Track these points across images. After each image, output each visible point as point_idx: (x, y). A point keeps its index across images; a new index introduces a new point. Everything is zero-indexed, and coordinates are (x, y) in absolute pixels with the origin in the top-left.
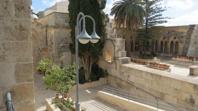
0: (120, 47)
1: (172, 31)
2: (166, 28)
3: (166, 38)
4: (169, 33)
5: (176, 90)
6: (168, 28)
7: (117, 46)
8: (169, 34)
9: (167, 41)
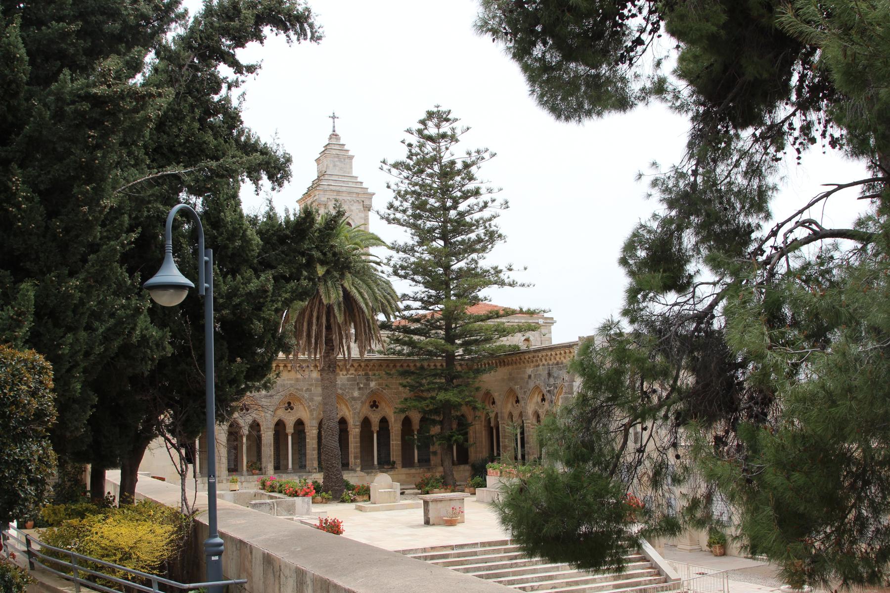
4: (549, 375)
8: (552, 381)
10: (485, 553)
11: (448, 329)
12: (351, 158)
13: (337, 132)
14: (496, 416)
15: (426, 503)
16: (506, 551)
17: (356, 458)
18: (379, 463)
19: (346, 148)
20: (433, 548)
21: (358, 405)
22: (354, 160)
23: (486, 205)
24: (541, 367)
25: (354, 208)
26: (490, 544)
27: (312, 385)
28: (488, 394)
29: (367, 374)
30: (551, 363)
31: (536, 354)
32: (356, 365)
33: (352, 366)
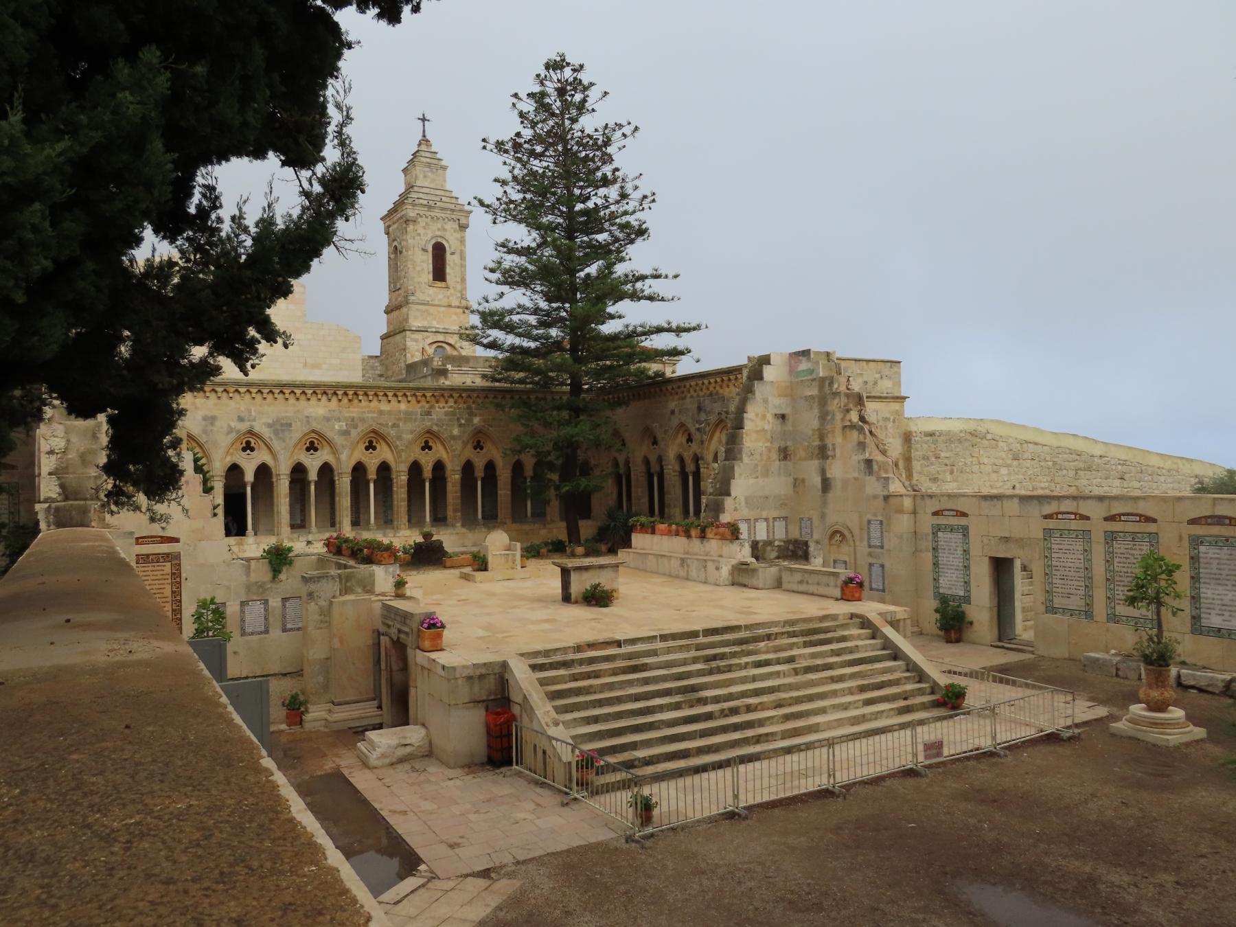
4: (700, 409)
7: (51, 452)
8: (703, 416)
10: (669, 650)
11: (573, 350)
12: (444, 168)
13: (428, 137)
14: (627, 462)
15: (565, 573)
16: (699, 647)
17: (455, 511)
18: (483, 518)
19: (438, 156)
20: (591, 646)
21: (458, 446)
22: (448, 172)
24: (688, 400)
25: (447, 227)
26: (674, 637)
27: (399, 419)
28: (616, 433)
29: (469, 408)
31: (682, 384)
32: (456, 395)
33: (451, 396)
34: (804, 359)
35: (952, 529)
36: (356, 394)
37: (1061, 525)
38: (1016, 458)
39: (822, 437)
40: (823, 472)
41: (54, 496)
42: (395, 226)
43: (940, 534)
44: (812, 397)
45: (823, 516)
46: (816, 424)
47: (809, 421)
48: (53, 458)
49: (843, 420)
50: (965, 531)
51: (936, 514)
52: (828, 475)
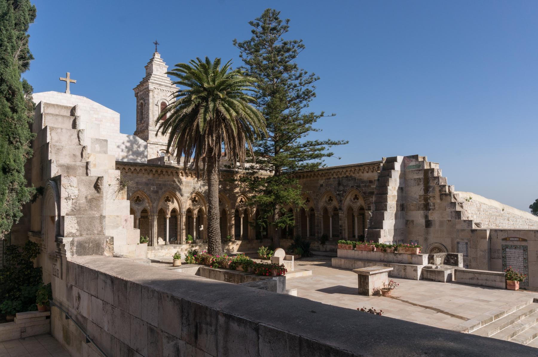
0: (83, 201)
1: (347, 177)
2: (332, 172)
3: (334, 199)
4: (339, 184)
5: (152, 330)
6: (336, 171)
8: (341, 188)
9: (338, 207)
23: (300, 76)
30: (340, 176)
34: (414, 160)
35: (516, 247)
36: (162, 172)
37: (511, 243)
38: (478, 211)
39: (426, 199)
40: (426, 217)
41: (74, 231)
42: (141, 93)
43: (507, 250)
44: (420, 179)
45: (426, 239)
46: (422, 193)
47: (417, 191)
48: (70, 202)
49: (440, 191)
50: (525, 249)
51: (503, 239)
52: (430, 219)
